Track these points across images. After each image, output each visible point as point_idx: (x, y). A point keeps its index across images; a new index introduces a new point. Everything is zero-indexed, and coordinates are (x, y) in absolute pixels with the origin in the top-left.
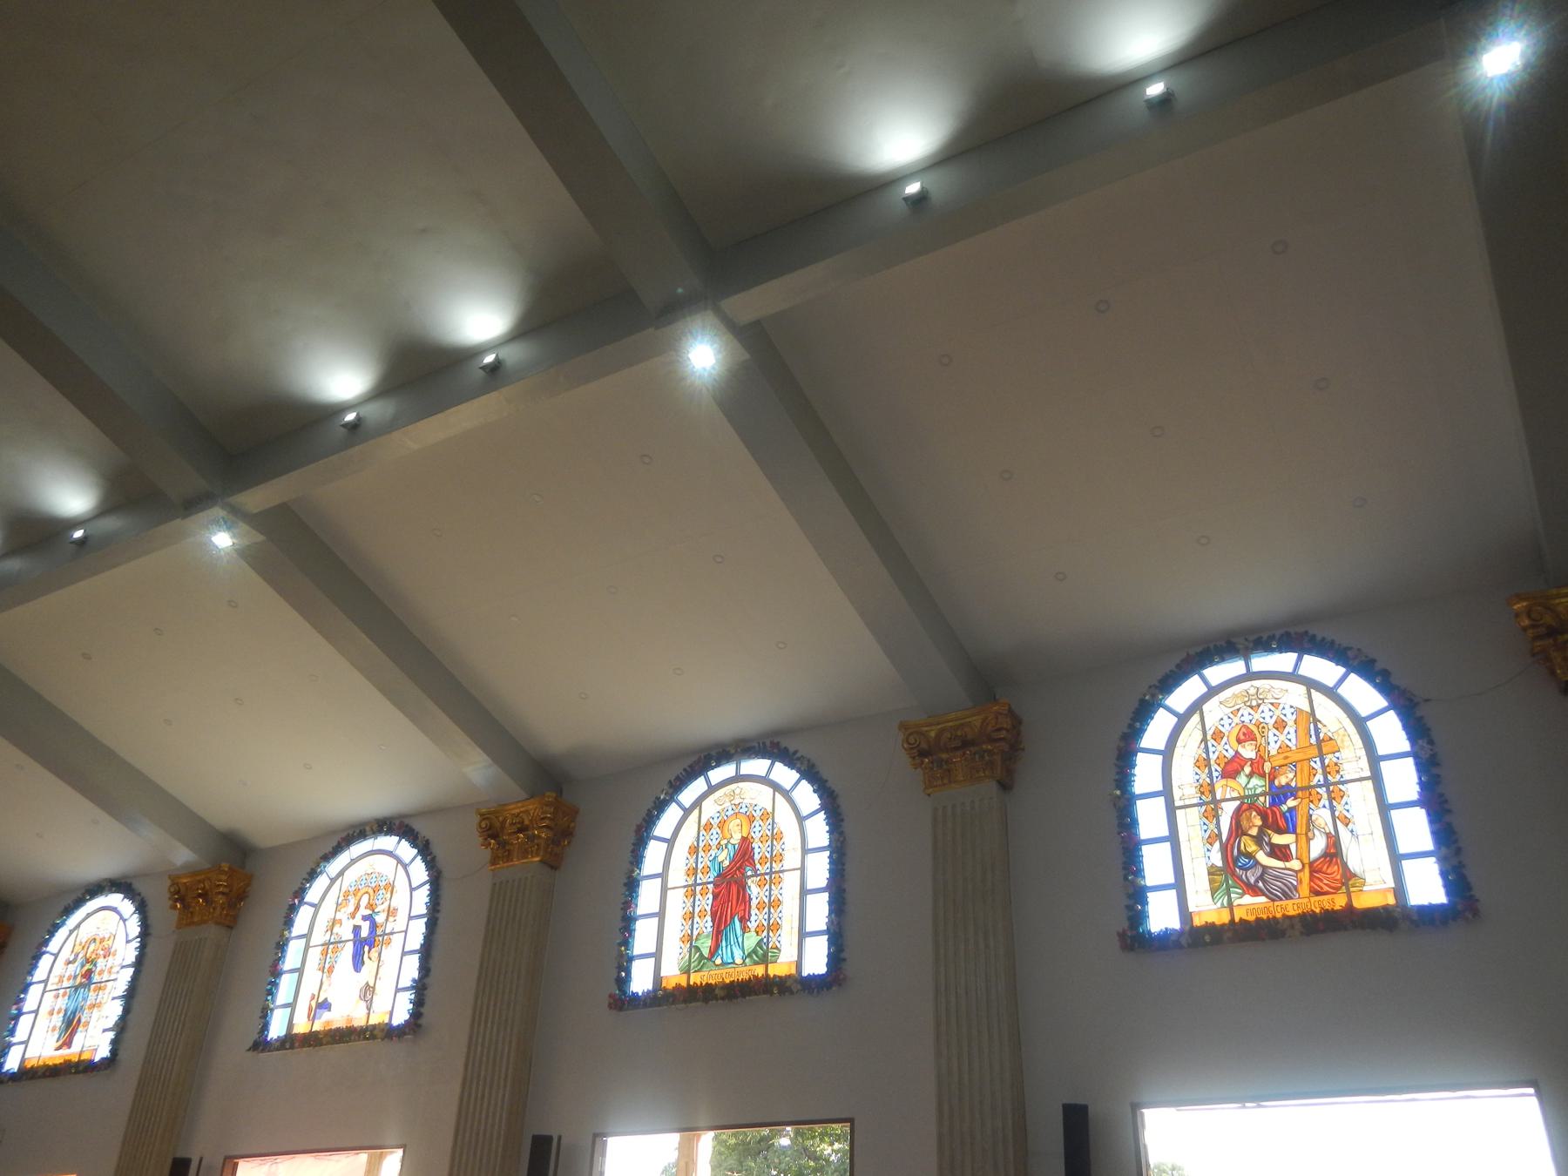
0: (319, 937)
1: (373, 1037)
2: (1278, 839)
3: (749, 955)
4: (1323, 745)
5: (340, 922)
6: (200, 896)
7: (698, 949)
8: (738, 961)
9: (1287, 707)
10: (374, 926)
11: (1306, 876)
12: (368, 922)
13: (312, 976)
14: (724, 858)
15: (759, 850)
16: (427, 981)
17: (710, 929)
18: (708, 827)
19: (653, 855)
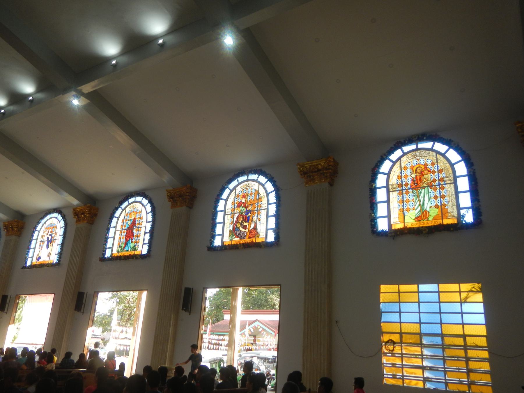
0: (39, 240)
1: (48, 266)
2: (245, 224)
3: (132, 249)
4: (259, 200)
5: (44, 236)
6: (10, 228)
7: (121, 247)
8: (129, 250)
9: (254, 189)
10: (52, 237)
11: (248, 233)
12: (50, 236)
13: (37, 249)
14: (130, 223)
15: (137, 221)
16: (62, 252)
17: (124, 242)
18: (127, 215)
19: (221, 205)
